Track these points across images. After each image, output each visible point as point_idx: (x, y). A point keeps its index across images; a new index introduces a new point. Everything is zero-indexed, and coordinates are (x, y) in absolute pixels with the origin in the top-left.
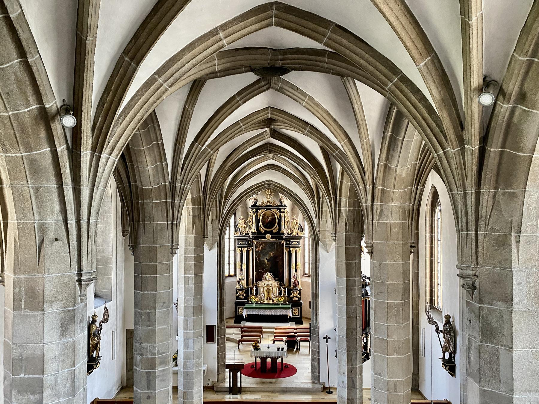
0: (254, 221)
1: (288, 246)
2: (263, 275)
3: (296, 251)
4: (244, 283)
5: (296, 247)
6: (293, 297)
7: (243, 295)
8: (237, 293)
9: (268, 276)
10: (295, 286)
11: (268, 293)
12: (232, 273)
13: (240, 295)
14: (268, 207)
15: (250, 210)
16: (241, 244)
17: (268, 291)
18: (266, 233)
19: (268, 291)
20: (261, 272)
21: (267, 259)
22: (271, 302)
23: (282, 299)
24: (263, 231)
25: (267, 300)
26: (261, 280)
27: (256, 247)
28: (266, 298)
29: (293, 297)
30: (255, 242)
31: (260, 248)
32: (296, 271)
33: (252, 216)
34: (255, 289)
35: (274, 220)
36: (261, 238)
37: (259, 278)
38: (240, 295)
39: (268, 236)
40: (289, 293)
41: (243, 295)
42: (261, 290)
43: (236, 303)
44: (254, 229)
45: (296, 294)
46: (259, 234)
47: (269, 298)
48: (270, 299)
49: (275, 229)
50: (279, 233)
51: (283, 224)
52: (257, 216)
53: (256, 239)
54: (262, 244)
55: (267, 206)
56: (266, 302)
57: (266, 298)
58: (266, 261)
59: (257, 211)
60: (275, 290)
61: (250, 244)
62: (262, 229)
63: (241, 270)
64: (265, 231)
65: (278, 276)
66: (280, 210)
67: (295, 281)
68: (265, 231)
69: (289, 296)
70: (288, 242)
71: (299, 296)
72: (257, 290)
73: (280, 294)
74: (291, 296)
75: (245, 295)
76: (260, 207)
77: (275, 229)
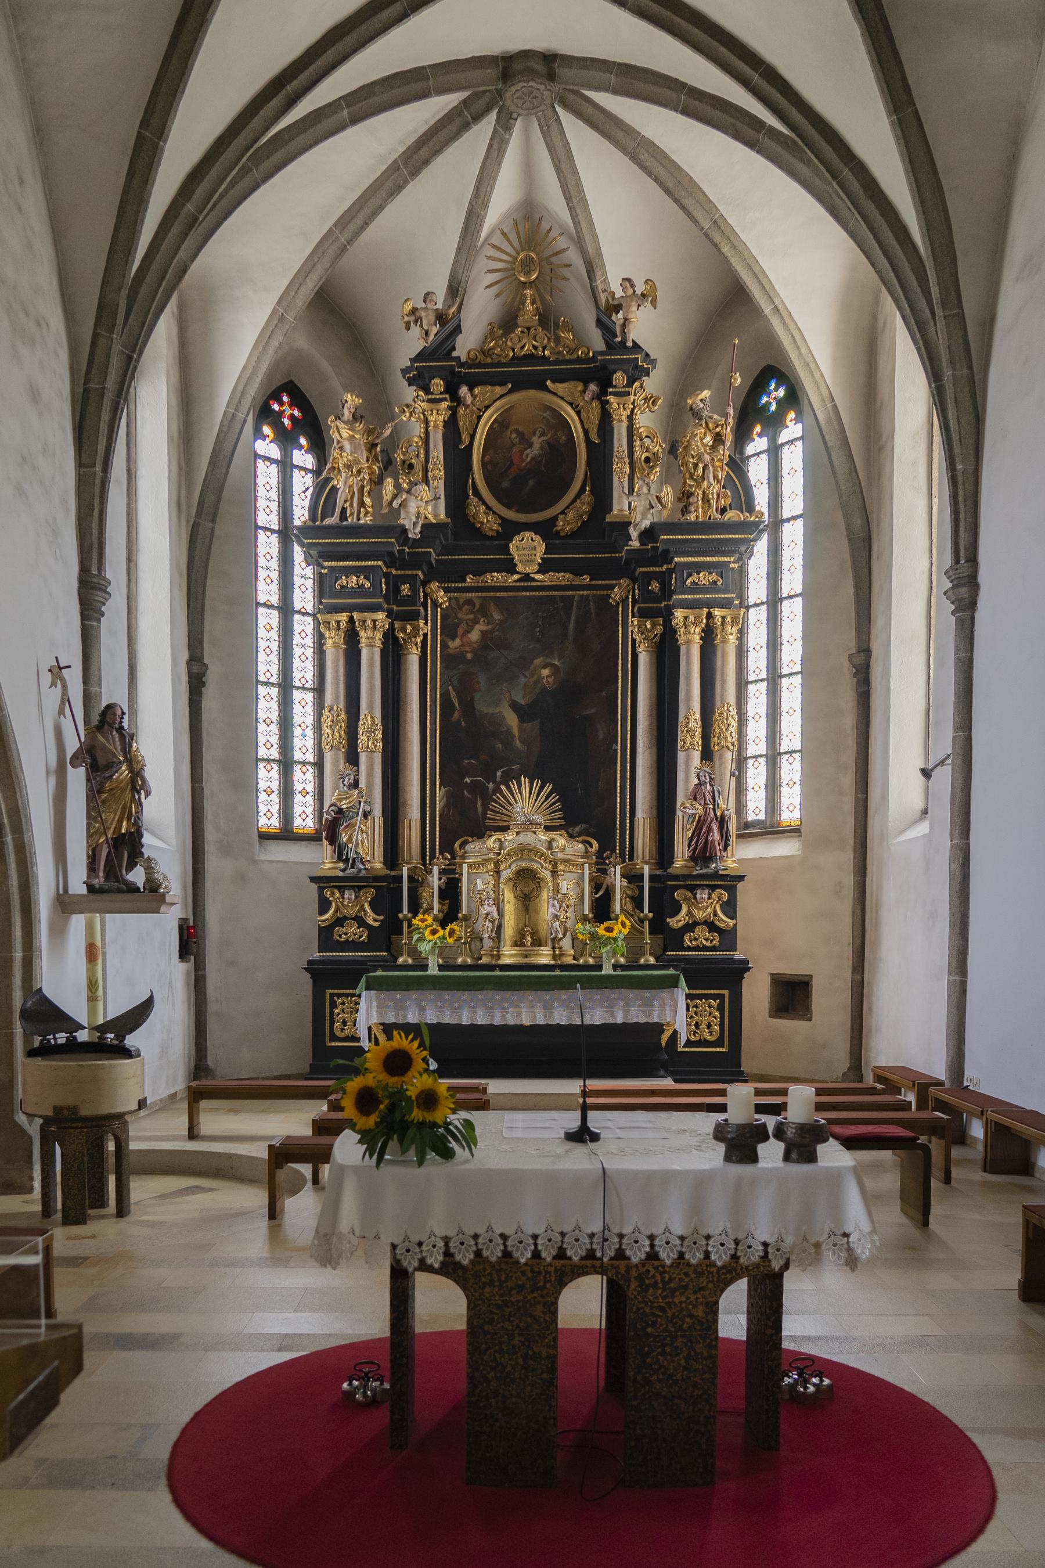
0: (437, 453)
1: (657, 608)
2: (487, 798)
3: (709, 635)
4: (366, 842)
5: (710, 604)
6: (690, 927)
7: (361, 921)
8: (324, 906)
9: (526, 801)
10: (703, 855)
11: (527, 901)
12: (304, 819)
13: (340, 921)
14: (527, 375)
15: (410, 393)
16: (345, 591)
17: (527, 885)
18: (510, 529)
19: (527, 885)
20: (474, 787)
21: (515, 707)
22: (544, 956)
23: (621, 928)
24: (489, 523)
25: (519, 943)
26: (480, 834)
27: (450, 631)
28: (509, 931)
29: (690, 927)
30: (441, 597)
31: (475, 636)
32: (707, 755)
33: (420, 417)
34: (435, 881)
35: (560, 451)
36: (480, 569)
37: (467, 818)
38: (340, 921)
40: (664, 903)
41: (361, 921)
42: (476, 883)
43: (314, 969)
45: (707, 905)
46: (461, 545)
47: (529, 935)
48: (538, 942)
49: (570, 512)
50: (602, 526)
51: (620, 468)
52: (451, 425)
53: (449, 574)
54: (484, 612)
55: (516, 360)
56: (509, 955)
57: (509, 931)
58: (512, 720)
59: (452, 390)
61: (412, 600)
63: (352, 758)
64: (504, 522)
65: (587, 809)
66: (605, 384)
67: (701, 825)
68: (504, 522)
69: (658, 926)
70: (655, 586)
71: (725, 921)
72: (451, 892)
73: (602, 911)
74: (676, 922)
75: (372, 918)
77: (570, 512)
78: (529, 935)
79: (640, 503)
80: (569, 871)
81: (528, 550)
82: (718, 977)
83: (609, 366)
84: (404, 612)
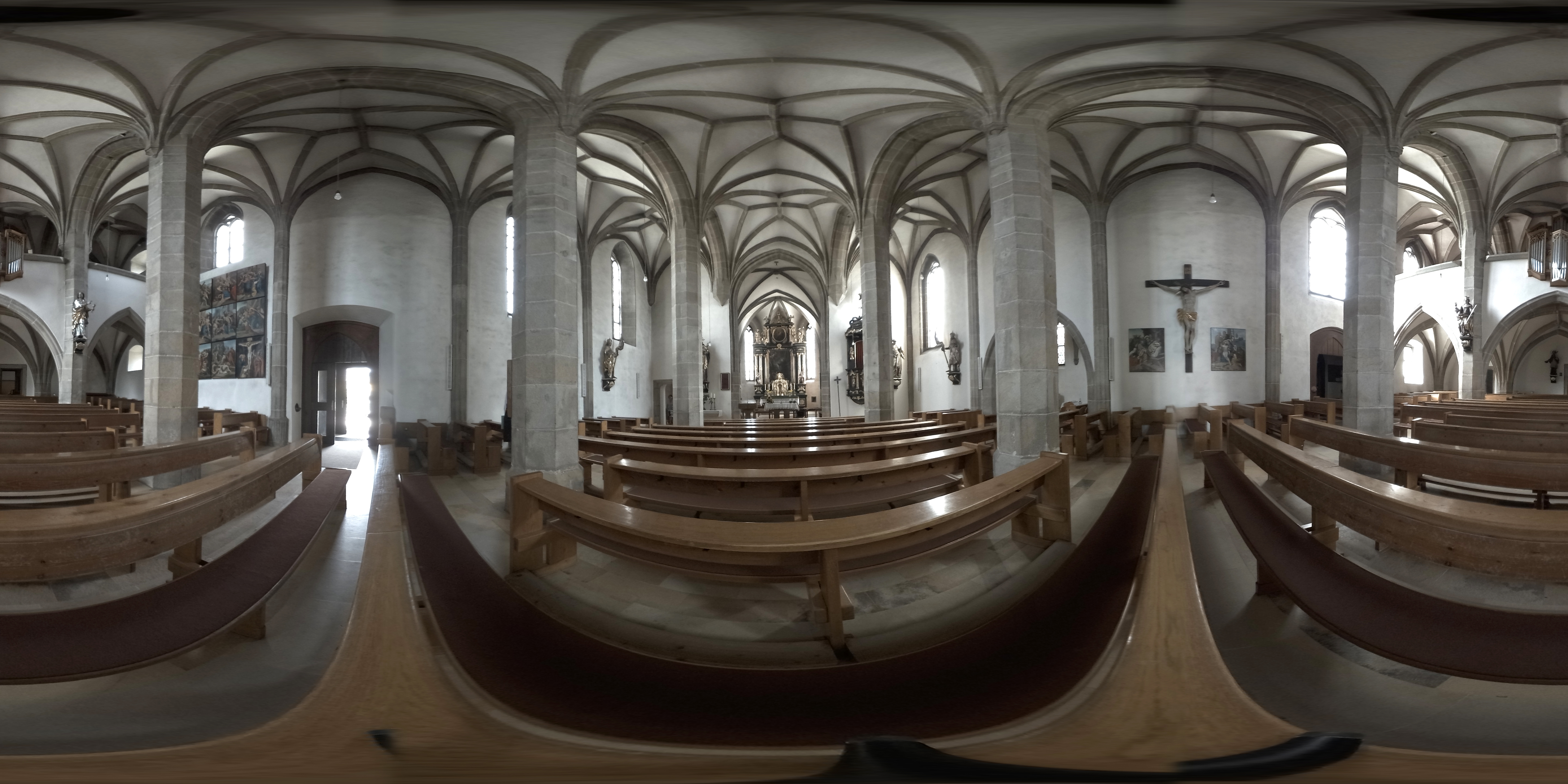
1: (795, 352)
4: (760, 381)
9: (780, 375)
14: (779, 325)
17: (780, 386)
33: (766, 330)
35: (783, 334)
37: (773, 378)
39: (779, 346)
44: (767, 341)
46: (771, 345)
47: (781, 392)
49: (784, 341)
50: (788, 343)
53: (770, 348)
60: (786, 386)
62: (774, 341)
65: (787, 377)
73: (789, 389)
76: (773, 325)
77: (784, 341)
78: (781, 392)
79: (793, 341)
80: (785, 384)
81: (779, 346)
82: (803, 397)
83: (789, 324)
84: (765, 353)
